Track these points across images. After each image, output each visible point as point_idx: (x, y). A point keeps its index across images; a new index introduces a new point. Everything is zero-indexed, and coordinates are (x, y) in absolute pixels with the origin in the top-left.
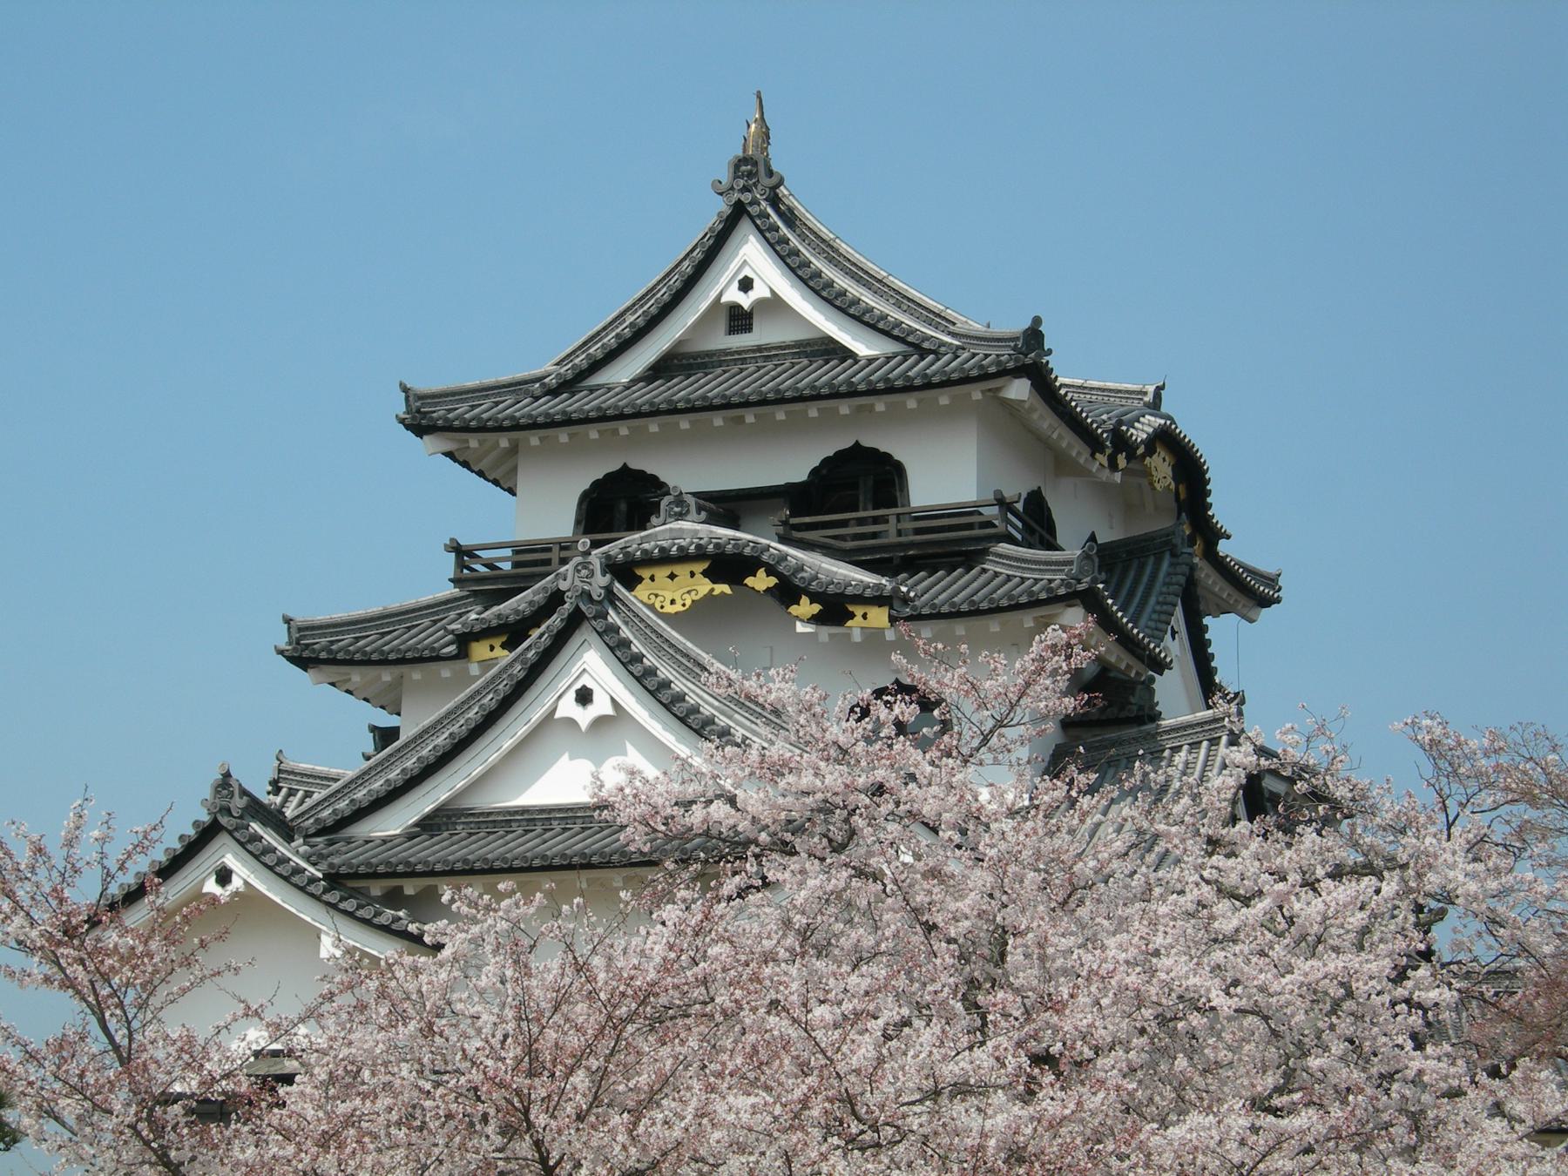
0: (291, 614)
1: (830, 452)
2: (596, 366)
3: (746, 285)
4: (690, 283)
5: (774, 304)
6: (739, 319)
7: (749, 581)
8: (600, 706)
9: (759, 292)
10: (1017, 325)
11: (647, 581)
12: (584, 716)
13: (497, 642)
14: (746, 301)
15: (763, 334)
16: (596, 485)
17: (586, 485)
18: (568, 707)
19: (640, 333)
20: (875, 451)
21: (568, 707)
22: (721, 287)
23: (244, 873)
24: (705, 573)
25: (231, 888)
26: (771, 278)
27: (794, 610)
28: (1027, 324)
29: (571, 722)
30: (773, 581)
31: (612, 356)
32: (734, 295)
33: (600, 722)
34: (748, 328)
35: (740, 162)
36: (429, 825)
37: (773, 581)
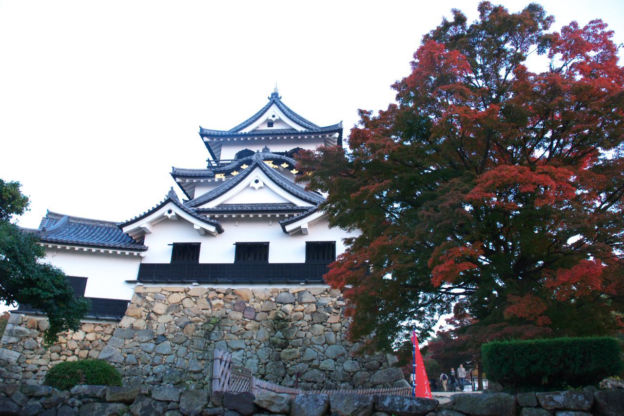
0: (174, 166)
1: (292, 149)
2: (241, 129)
3: (274, 116)
4: (262, 114)
5: (279, 121)
6: (270, 124)
7: (282, 165)
9: (277, 118)
13: (223, 175)
14: (274, 119)
15: (276, 127)
16: (240, 152)
17: (238, 152)
19: (251, 123)
22: (268, 115)
23: (176, 210)
24: (272, 163)
25: (171, 214)
26: (279, 115)
27: (292, 172)
30: (287, 166)
31: (245, 127)
32: (270, 118)
35: (273, 94)
37: (287, 166)
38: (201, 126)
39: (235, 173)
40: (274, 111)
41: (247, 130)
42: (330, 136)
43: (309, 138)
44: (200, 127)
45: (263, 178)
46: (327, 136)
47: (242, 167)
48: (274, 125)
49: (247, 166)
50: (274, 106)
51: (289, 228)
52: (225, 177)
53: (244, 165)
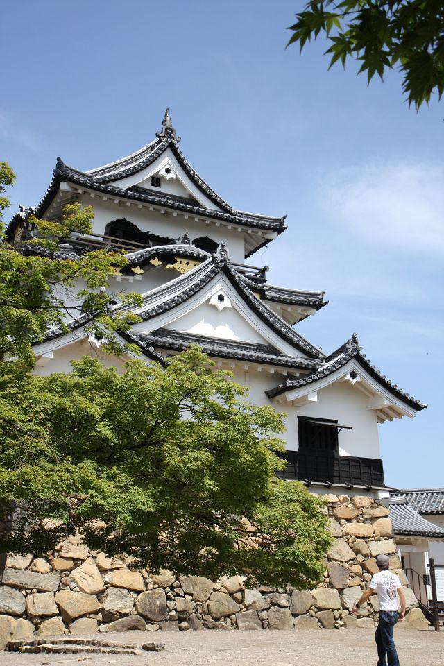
2: (117, 178)
5: (175, 182)
6: (156, 180)
8: (227, 303)
9: (172, 175)
10: (280, 217)
11: (178, 263)
12: (221, 306)
13: (118, 269)
15: (163, 189)
16: (113, 222)
17: (110, 221)
18: (214, 301)
20: (212, 241)
21: (214, 301)
26: (176, 173)
28: (284, 216)
29: (214, 307)
32: (163, 173)
33: (225, 309)
34: (159, 186)
36: (154, 333)
38: (62, 160)
39: (138, 270)
40: (167, 161)
41: (123, 185)
42: (263, 233)
43: (167, 214)
44: (59, 159)
45: (232, 299)
46: (260, 234)
47: (152, 261)
48: (162, 185)
49: (160, 263)
50: (169, 152)
51: (291, 396)
52: (121, 274)
53: (156, 259)
